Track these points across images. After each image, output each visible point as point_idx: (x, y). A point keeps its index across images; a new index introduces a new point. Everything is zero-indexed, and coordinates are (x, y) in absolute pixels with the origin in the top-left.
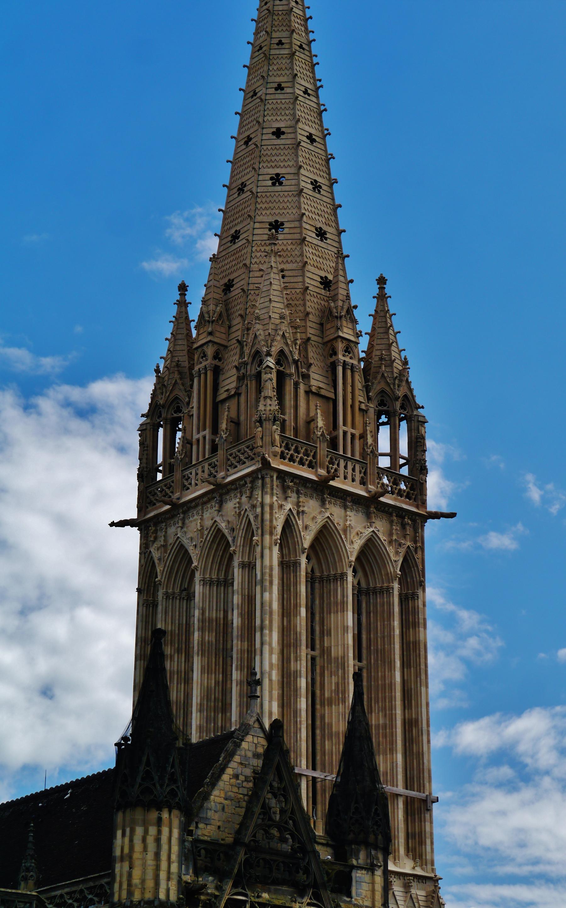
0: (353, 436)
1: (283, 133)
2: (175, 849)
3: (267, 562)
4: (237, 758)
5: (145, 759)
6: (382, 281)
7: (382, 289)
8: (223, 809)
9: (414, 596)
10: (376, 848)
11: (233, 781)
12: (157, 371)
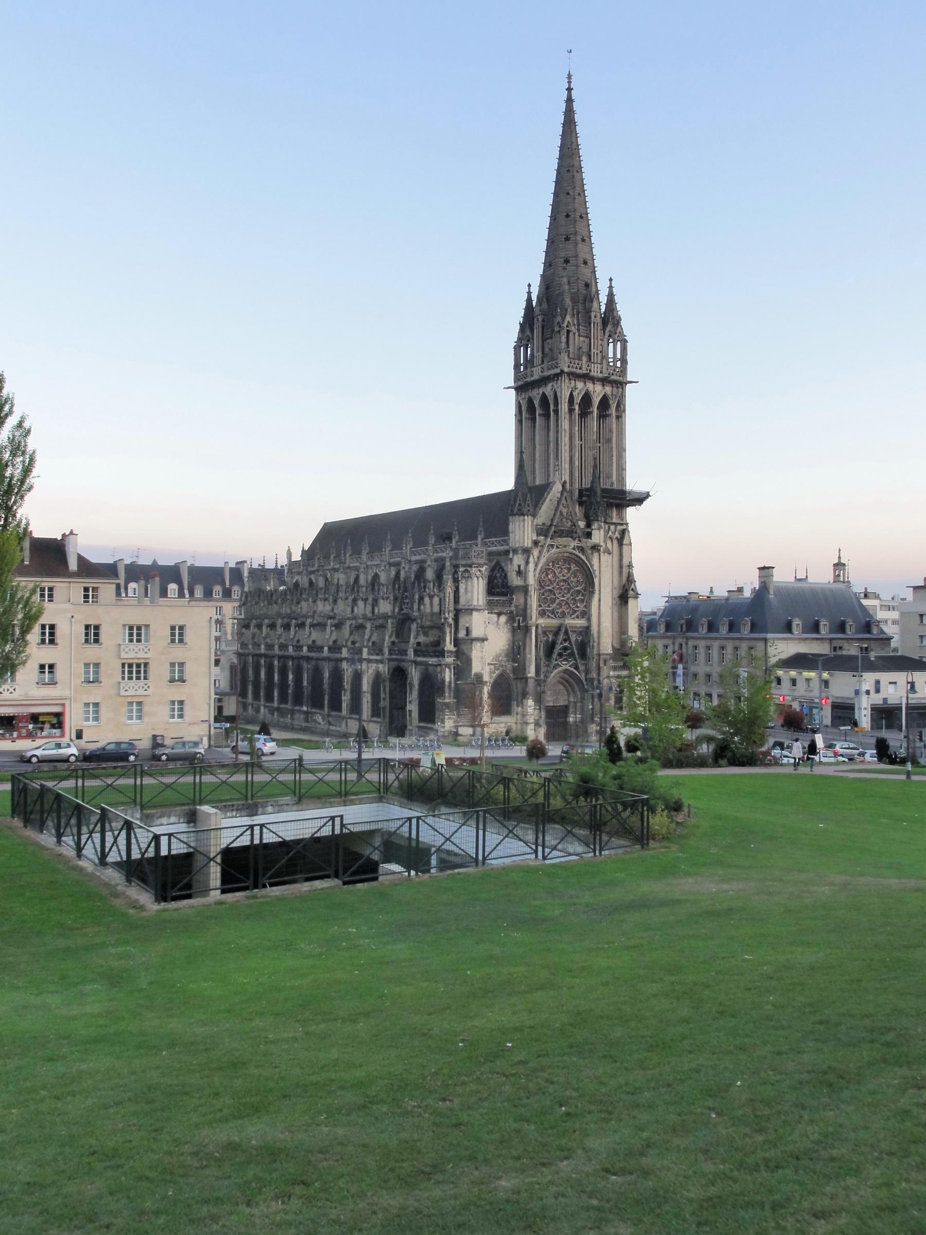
2: (530, 529)
4: (551, 494)
6: (611, 280)
7: (611, 283)
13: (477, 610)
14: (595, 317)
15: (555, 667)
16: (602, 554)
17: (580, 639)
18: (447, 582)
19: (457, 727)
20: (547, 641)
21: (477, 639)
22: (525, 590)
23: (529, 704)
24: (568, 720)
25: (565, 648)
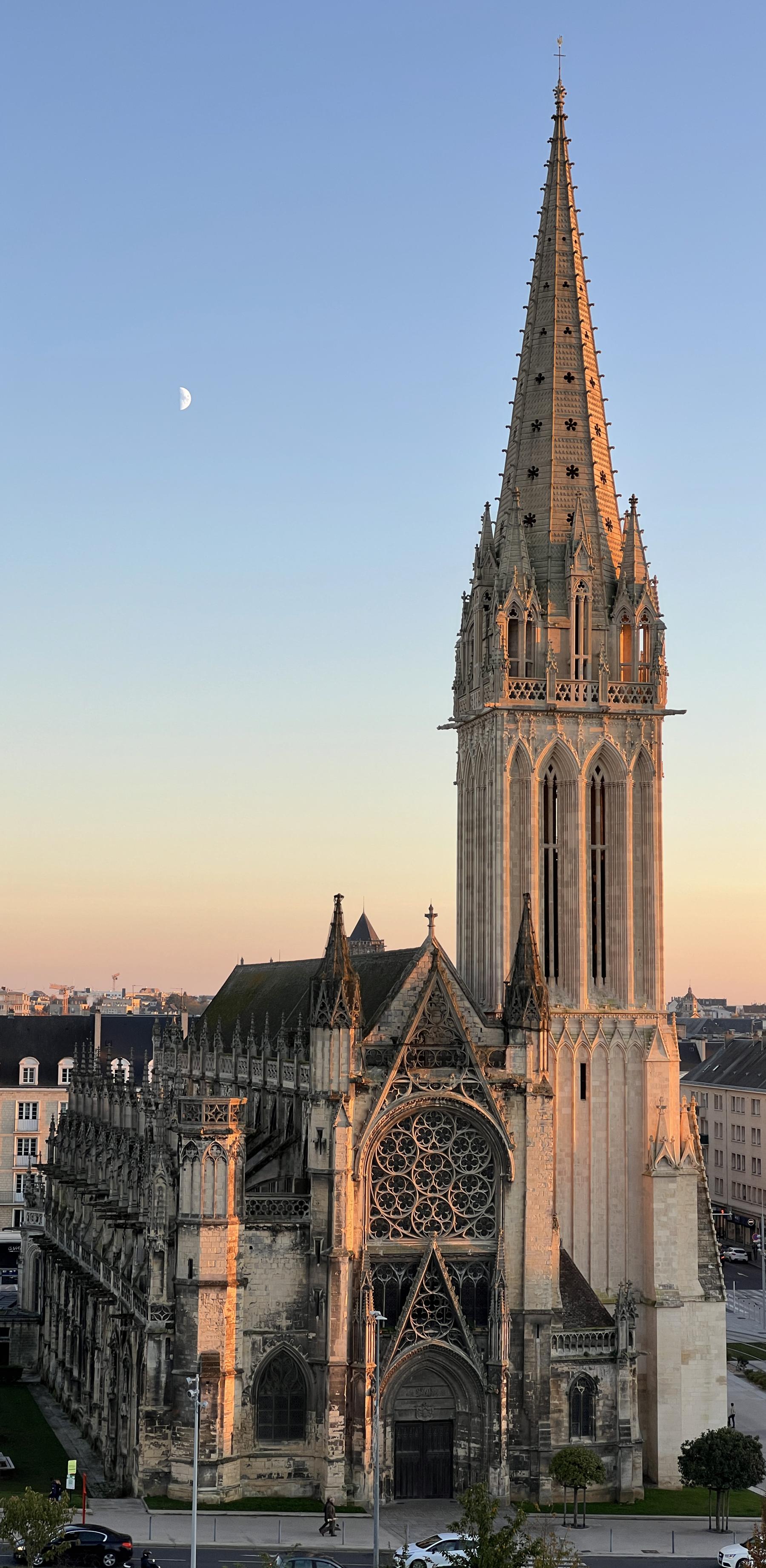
0: (585, 661)
1: (543, 378)
2: (344, 1055)
3: (499, 787)
5: (321, 995)
6: (633, 501)
7: (633, 508)
8: (402, 1014)
9: (649, 785)
10: (530, 1030)
11: (412, 993)
12: (464, 598)
13: (207, 1225)
14: (581, 585)
15: (404, 1343)
16: (528, 1099)
17: (475, 1280)
18: (155, 1168)
19: (167, 1462)
20: (392, 1286)
21: (210, 1285)
22: (328, 1178)
23: (332, 1420)
24: (455, 1453)
25: (432, 1302)
